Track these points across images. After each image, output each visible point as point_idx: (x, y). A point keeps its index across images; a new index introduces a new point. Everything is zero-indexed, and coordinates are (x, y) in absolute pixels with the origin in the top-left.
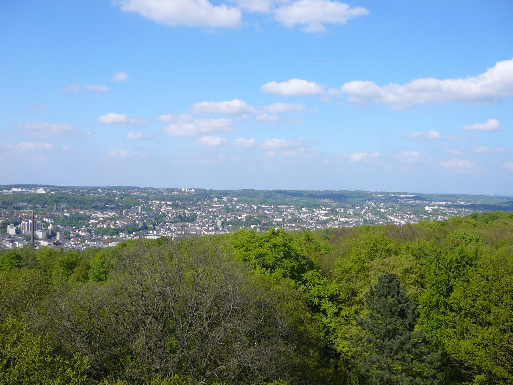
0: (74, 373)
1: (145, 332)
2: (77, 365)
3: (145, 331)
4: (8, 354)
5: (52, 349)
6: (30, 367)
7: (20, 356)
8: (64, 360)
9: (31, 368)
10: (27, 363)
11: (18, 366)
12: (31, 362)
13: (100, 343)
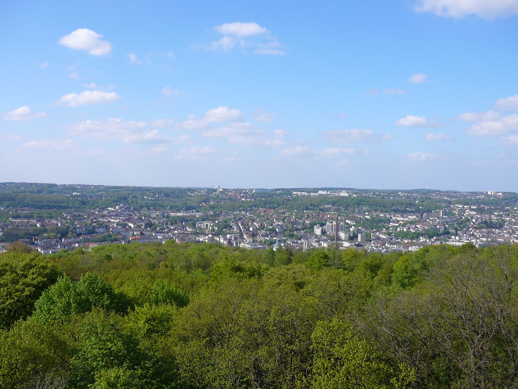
0: (400, 383)
1: (473, 351)
2: (402, 376)
3: (473, 350)
4: (336, 354)
5: (376, 355)
6: (357, 370)
7: (347, 357)
8: (388, 368)
9: (358, 371)
10: (354, 365)
11: (346, 367)
12: (358, 365)
13: (420, 355)
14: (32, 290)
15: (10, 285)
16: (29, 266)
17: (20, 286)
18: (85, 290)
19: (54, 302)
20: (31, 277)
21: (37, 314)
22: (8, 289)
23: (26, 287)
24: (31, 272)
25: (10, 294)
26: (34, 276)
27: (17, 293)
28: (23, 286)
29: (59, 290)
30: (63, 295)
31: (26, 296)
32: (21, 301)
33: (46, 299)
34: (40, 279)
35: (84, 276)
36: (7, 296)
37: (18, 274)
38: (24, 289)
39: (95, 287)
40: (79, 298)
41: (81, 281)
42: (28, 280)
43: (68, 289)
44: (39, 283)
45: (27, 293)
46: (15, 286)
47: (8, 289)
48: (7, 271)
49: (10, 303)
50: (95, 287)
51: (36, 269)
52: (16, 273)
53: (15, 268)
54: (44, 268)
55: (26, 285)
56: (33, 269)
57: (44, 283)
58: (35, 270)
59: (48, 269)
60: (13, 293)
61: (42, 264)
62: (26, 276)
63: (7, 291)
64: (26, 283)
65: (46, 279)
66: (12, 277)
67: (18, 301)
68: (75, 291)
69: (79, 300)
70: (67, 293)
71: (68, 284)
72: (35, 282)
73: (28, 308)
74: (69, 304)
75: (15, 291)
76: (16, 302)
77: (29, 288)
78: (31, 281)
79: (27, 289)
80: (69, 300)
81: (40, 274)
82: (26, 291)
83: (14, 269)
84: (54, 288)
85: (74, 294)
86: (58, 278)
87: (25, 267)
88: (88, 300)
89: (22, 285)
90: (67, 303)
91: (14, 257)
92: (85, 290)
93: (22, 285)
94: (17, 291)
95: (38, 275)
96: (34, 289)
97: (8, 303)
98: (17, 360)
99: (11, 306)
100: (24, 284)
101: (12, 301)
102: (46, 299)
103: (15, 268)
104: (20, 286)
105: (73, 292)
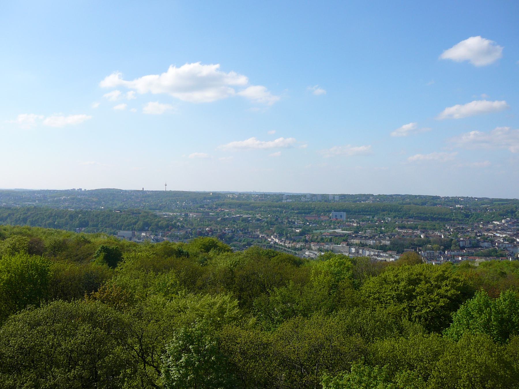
14: (447, 301)
15: (425, 294)
16: (442, 278)
17: (435, 297)
18: (505, 308)
19: (472, 317)
20: (445, 288)
21: (455, 327)
22: (424, 298)
23: (441, 298)
24: (444, 284)
25: (426, 303)
26: (449, 288)
27: (432, 303)
28: (437, 297)
29: (478, 306)
30: (482, 311)
31: (441, 307)
32: (436, 312)
33: (465, 313)
34: (452, 291)
35: (504, 294)
36: (422, 304)
37: (432, 285)
38: (438, 299)
39: (517, 306)
40: (500, 316)
41: (501, 298)
42: (442, 291)
43: (487, 305)
44: (453, 295)
45: (441, 304)
46: (430, 295)
47: (424, 298)
48: (421, 280)
49: (426, 312)
50: (517, 306)
51: (450, 281)
52: (430, 282)
53: (429, 278)
54: (455, 280)
55: (440, 296)
56: (446, 281)
57: (457, 296)
58: (448, 282)
59: (461, 283)
60: (429, 302)
61: (454, 276)
62: (439, 288)
63: (423, 300)
64: (440, 294)
65: (459, 292)
66: (427, 286)
67: (433, 310)
68: (495, 308)
69: (500, 318)
70: (487, 310)
71: (487, 300)
72: (449, 294)
73: (442, 319)
74: (489, 320)
75: (430, 301)
76: (431, 312)
77: (444, 299)
78: (444, 293)
79: (442, 300)
80: (490, 317)
81: (453, 287)
82: (441, 301)
83: (427, 279)
84: (473, 303)
85: (495, 311)
86: (476, 293)
87: (438, 277)
88: (509, 320)
89: (436, 295)
90: (487, 319)
91: (426, 267)
92: (505, 308)
93: (436, 295)
94: (432, 300)
95: (451, 287)
96: (449, 300)
97: (425, 311)
98: (476, 374)
99: (428, 315)
100: (438, 295)
101: (428, 310)
102: (465, 313)
103: (429, 278)
104: (435, 297)
105: (493, 309)
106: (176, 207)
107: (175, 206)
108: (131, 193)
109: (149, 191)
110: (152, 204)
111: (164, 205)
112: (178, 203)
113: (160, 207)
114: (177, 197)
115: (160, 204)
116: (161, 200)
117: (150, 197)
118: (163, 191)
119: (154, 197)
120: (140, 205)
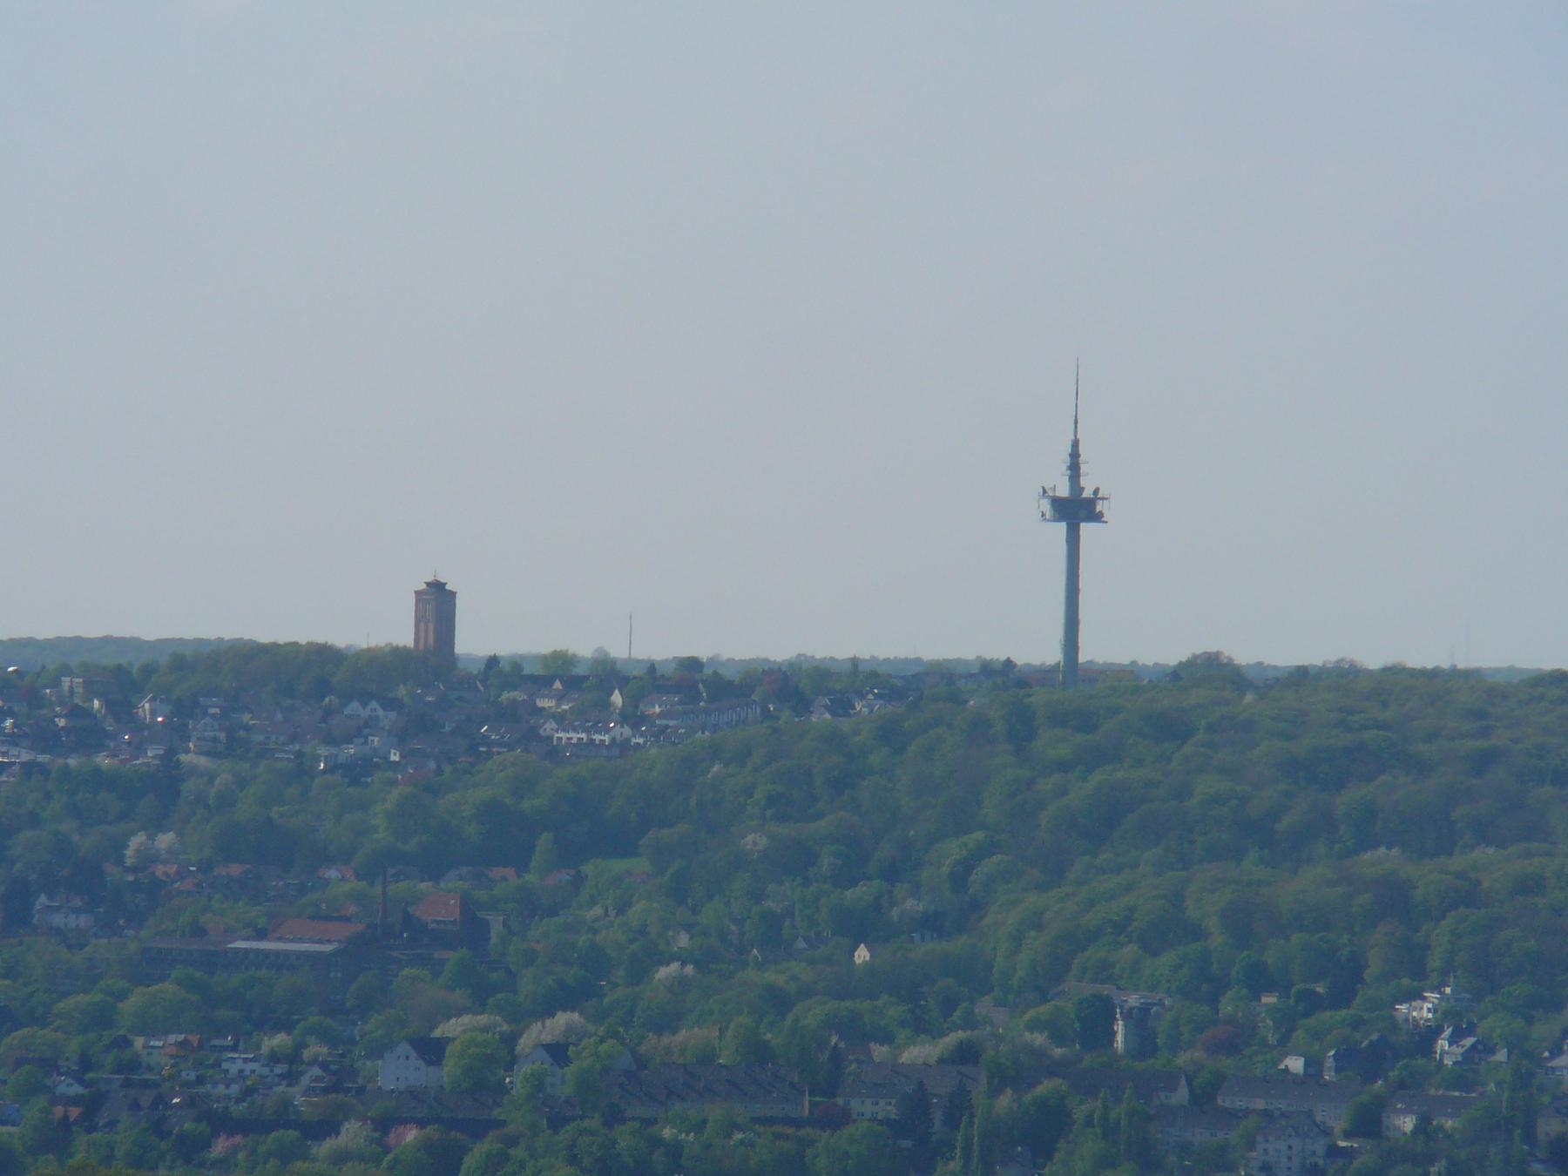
106: (1368, 1123)
107: (1337, 1117)
108: (88, 735)
109: (607, 675)
110: (687, 1037)
111: (1013, 1076)
112: (1423, 1011)
113: (917, 1105)
114: (1382, 860)
115: (918, 1053)
116: (932, 924)
117: (620, 842)
118: (1000, 675)
119: (754, 841)
120: (340, 1079)
